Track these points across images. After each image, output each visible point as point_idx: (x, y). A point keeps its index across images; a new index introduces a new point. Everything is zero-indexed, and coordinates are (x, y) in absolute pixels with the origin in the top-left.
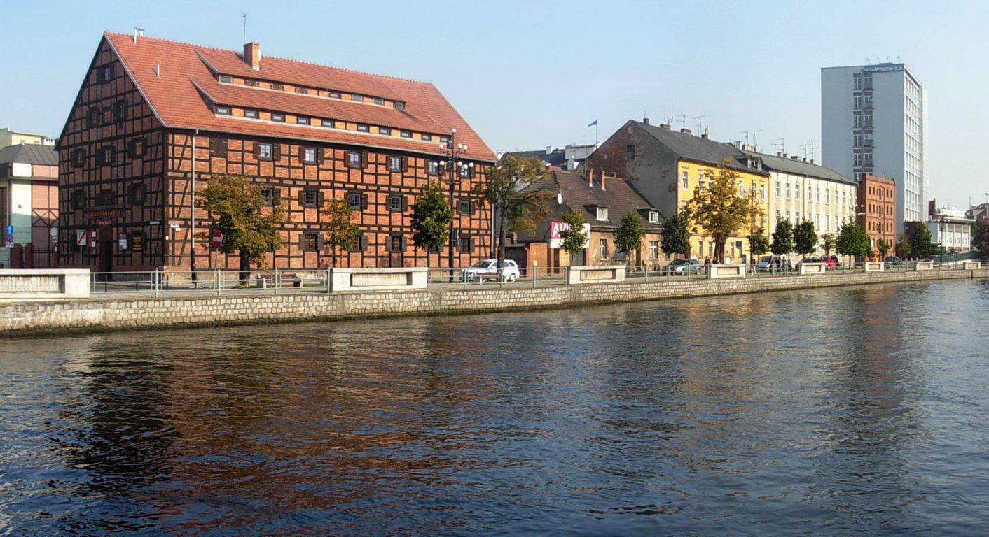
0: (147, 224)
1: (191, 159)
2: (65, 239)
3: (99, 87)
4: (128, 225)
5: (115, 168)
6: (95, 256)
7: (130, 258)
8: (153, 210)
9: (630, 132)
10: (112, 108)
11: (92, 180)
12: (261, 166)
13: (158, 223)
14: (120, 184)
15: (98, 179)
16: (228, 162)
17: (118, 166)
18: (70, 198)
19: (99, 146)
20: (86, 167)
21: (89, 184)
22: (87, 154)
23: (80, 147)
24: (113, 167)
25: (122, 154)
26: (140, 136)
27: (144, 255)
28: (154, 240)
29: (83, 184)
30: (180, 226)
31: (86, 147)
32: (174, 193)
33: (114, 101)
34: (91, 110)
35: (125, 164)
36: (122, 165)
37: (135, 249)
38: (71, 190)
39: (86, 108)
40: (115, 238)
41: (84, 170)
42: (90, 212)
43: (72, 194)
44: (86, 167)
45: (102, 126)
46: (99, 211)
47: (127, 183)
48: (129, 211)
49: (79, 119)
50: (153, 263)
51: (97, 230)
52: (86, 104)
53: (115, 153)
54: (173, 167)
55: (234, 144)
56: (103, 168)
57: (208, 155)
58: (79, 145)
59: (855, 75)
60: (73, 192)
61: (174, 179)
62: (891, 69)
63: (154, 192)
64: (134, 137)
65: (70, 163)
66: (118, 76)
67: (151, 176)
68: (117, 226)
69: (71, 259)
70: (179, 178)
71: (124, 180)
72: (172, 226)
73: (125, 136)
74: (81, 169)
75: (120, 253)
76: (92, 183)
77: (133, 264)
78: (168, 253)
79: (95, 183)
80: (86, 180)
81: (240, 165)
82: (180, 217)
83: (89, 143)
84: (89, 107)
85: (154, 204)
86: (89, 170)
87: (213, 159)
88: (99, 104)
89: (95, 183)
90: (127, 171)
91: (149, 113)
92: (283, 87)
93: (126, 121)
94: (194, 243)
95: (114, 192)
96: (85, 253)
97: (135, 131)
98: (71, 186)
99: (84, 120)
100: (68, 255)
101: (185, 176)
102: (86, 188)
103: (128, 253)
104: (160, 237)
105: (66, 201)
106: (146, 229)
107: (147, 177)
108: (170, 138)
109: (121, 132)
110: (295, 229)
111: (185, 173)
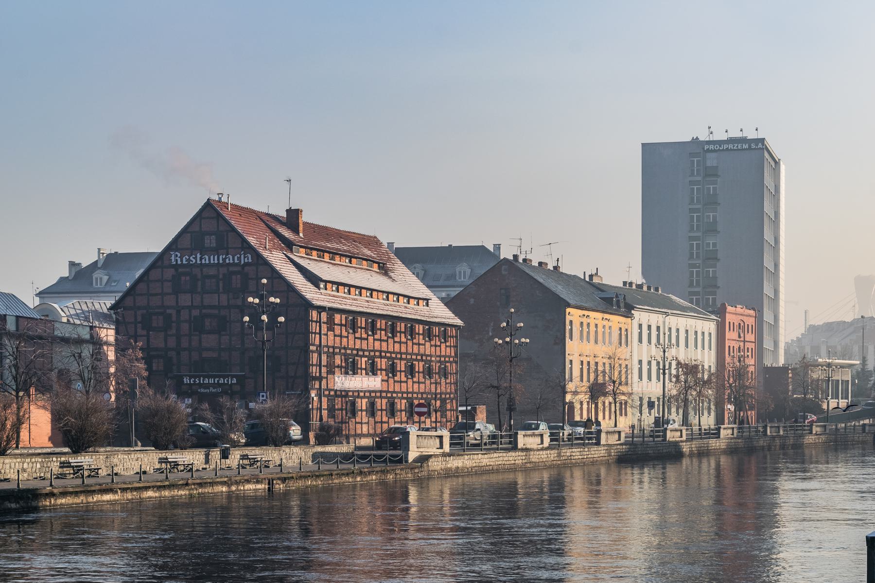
10: (221, 276)
11: (185, 343)
19: (196, 313)
20: (174, 331)
33: (223, 270)
39: (169, 273)
55: (337, 318)
56: (204, 336)
59: (692, 155)
61: (313, 352)
62: (746, 146)
84: (176, 270)
92: (323, 255)
102: (173, 354)
110: (364, 397)
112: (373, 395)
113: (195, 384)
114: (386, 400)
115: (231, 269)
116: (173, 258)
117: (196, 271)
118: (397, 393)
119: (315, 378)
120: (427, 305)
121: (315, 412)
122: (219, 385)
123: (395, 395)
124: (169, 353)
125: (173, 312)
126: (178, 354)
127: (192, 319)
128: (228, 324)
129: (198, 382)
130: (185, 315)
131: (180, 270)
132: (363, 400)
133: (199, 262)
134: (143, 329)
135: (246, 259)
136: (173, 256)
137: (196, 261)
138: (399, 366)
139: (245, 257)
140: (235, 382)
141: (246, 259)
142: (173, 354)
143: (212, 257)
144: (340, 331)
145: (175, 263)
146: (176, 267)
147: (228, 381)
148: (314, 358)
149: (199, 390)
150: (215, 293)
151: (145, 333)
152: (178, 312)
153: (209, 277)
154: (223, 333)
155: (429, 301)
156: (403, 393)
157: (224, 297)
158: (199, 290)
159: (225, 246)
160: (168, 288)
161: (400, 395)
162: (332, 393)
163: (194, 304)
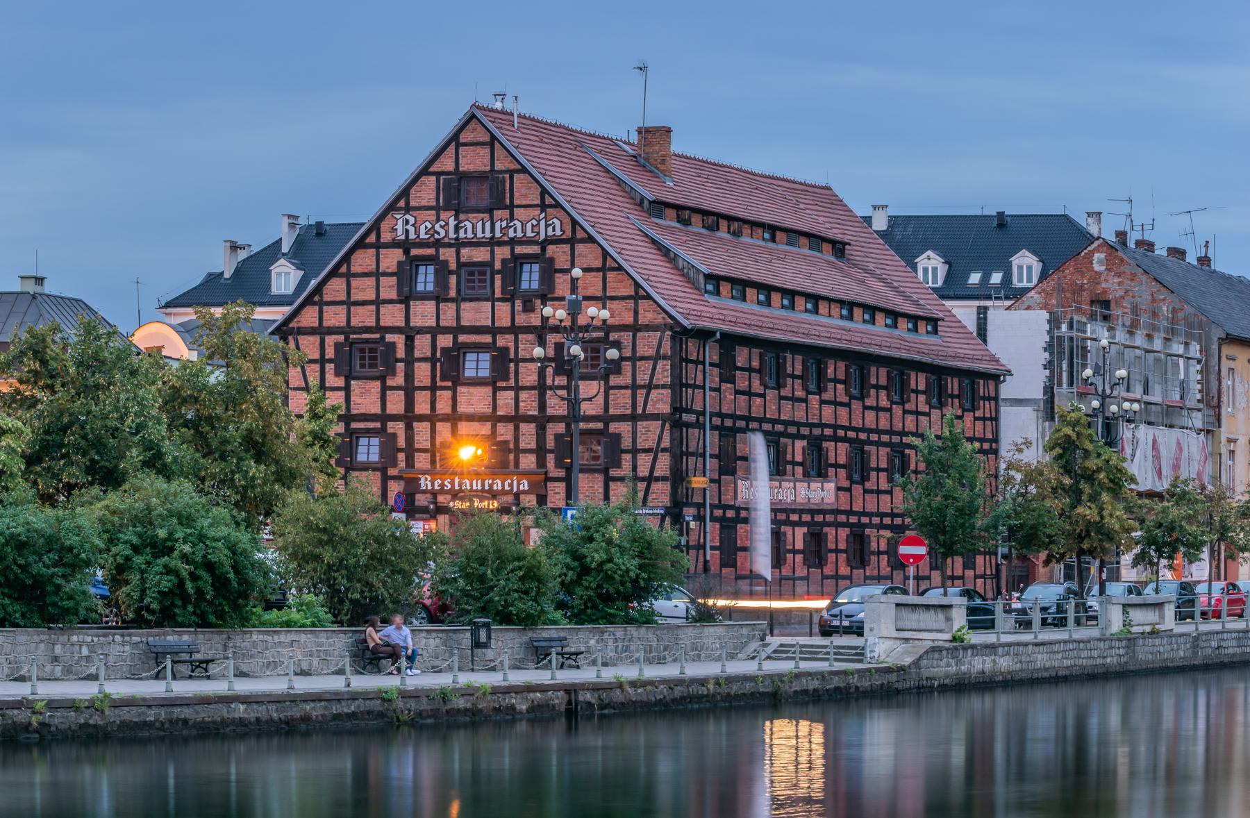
1: (703, 387)
8: (641, 486)
9: (1097, 267)
10: (498, 266)
11: (422, 407)
12: (768, 398)
13: (662, 512)
14: (528, 430)
17: (518, 389)
19: (445, 341)
20: (399, 380)
23: (377, 336)
26: (595, 335)
29: (384, 418)
33: (503, 253)
41: (384, 389)
45: (458, 300)
47: (550, 425)
51: (444, 519)
52: (395, 244)
53: (503, 363)
55: (742, 356)
56: (461, 390)
57: (717, 379)
61: (688, 425)
67: (633, 418)
72: (687, 518)
74: (378, 383)
81: (747, 397)
82: (695, 500)
84: (407, 252)
85: (643, 471)
86: (409, 390)
87: (724, 386)
94: (708, 552)
95: (506, 442)
102: (397, 428)
107: (621, 418)
109: (535, 321)
112: (819, 518)
113: (442, 491)
114: (847, 530)
115: (519, 250)
116: (399, 227)
117: (447, 254)
118: (870, 515)
120: (935, 331)
122: (494, 495)
124: (390, 424)
125: (399, 340)
126: (409, 428)
127: (438, 355)
128: (512, 365)
129: (449, 486)
130: (422, 345)
131: (414, 252)
133: (452, 235)
134: (337, 374)
135: (550, 229)
136: (400, 222)
137: (447, 232)
139: (547, 226)
140: (526, 488)
141: (550, 229)
142: (397, 428)
143: (480, 225)
144: (747, 383)
145: (403, 237)
146: (405, 245)
147: (511, 485)
149: (451, 504)
150: (487, 300)
151: (340, 382)
152: (410, 341)
154: (499, 384)
155: (939, 323)
156: (882, 515)
157: (503, 309)
158: (453, 293)
159: (508, 201)
160: (389, 288)
161: (876, 520)
162: (730, 514)
163: (442, 324)
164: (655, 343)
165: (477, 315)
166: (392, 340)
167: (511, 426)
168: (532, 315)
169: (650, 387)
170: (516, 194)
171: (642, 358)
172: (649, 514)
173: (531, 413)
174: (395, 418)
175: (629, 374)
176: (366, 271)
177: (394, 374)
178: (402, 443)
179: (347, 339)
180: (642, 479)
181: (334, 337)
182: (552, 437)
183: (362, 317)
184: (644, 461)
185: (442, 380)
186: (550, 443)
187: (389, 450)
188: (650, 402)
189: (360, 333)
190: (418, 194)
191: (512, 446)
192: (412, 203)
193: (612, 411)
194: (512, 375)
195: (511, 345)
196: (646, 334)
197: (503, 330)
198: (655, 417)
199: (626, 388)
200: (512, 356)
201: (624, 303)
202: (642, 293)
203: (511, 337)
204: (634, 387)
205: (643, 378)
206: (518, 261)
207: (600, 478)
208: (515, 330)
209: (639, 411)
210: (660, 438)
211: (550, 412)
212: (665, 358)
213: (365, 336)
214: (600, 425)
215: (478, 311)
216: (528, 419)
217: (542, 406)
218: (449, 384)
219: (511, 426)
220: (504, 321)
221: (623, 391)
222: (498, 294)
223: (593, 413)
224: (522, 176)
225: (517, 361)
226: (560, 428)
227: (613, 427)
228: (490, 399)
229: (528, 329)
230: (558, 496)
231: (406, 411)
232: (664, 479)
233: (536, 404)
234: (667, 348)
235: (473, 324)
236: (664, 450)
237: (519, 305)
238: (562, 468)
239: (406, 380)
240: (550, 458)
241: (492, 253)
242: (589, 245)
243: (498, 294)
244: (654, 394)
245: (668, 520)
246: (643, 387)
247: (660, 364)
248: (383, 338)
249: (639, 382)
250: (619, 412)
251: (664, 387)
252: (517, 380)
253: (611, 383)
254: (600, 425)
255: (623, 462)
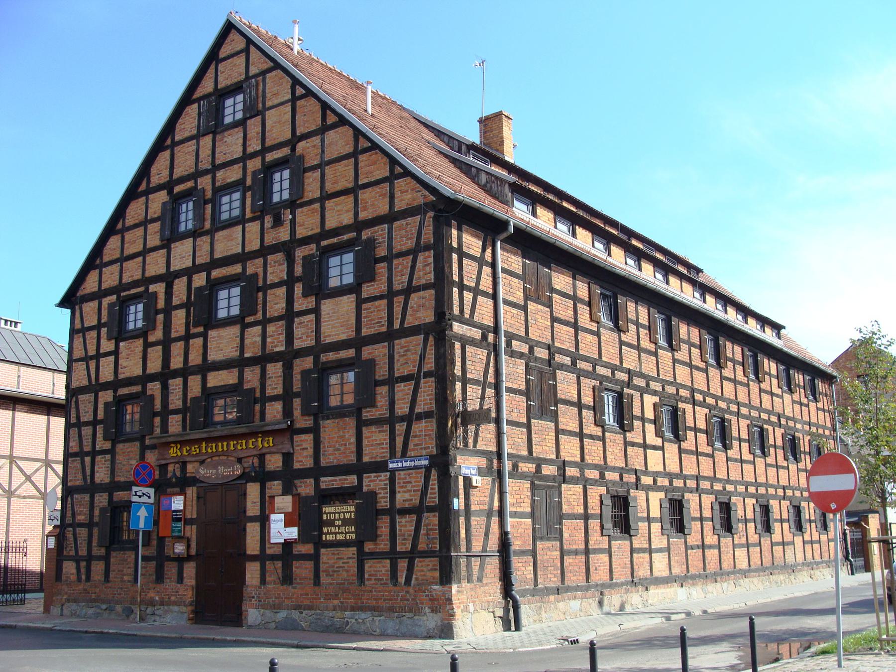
0: (379, 467)
2: (81, 518)
3: (207, 141)
4: (304, 474)
5: (258, 329)
6: (180, 560)
7: (310, 564)
8: (400, 428)
10: (249, 182)
11: (176, 362)
14: (275, 370)
15: (195, 358)
16: (554, 320)
17: (265, 322)
18: (101, 415)
19: (200, 280)
20: (157, 335)
21: (165, 375)
22: (161, 304)
23: (141, 289)
24: (245, 326)
25: (282, 291)
26: (345, 237)
27: (362, 558)
28: (404, 512)
29: (145, 379)
30: (480, 472)
31: (159, 288)
32: (465, 381)
33: (254, 164)
34: (177, 200)
35: (290, 316)
36: (279, 318)
37: (329, 537)
38: (107, 396)
40: (253, 509)
41: (147, 345)
42: (167, 445)
43: (107, 405)
44: (157, 335)
45: (211, 232)
46: (198, 441)
47: (297, 362)
48: (309, 438)
49: (136, 226)
50: (402, 580)
51: (191, 492)
52: (159, 188)
54: (462, 311)
56: (212, 334)
57: (521, 294)
58: (135, 284)
60: (110, 399)
63: (405, 379)
64: (324, 243)
65: (104, 330)
66: (269, 104)
67: (389, 336)
68: (263, 477)
69: (98, 568)
70: (473, 342)
71: (288, 358)
73: (287, 248)
74: (141, 341)
75: (269, 552)
76: (175, 374)
77: (324, 579)
78: (458, 549)
79: (185, 373)
80: (155, 365)
82: (481, 446)
83: (168, 278)
84: (170, 192)
85: (402, 408)
87: (531, 306)
88: (205, 182)
89: (185, 373)
90: (298, 332)
91: (382, 171)
93: (293, 204)
95: (253, 390)
96: (147, 553)
97: (331, 223)
98: (106, 386)
99: (154, 227)
100: (90, 558)
101: (484, 337)
102: (154, 388)
103: (308, 549)
104: (433, 497)
105: (87, 424)
106: (375, 482)
108: (454, 232)
109: (283, 234)
110: (655, 487)
111: (485, 330)
114: (712, 497)
117: (205, 182)
118: (735, 483)
119: (480, 417)
121: (477, 523)
123: (730, 488)
124: (150, 385)
125: (159, 288)
128: (260, 294)
132: (652, 494)
138: (734, 428)
148: (477, 359)
153: (229, 188)
156: (747, 485)
162: (549, 470)
164: (415, 231)
165: (229, 244)
166: (155, 290)
167: (257, 370)
168: (281, 229)
169: (409, 290)
170: (268, 95)
171: (401, 255)
172: (410, 468)
173: (277, 349)
174: (153, 378)
175: (385, 279)
176: (137, 221)
177: (154, 329)
178: (158, 406)
179: (118, 297)
180: (402, 419)
181: (109, 298)
182: (299, 377)
183: (133, 271)
184: (403, 391)
185: (195, 326)
186: (297, 386)
187: (148, 414)
188: (409, 312)
189: (129, 289)
190: (182, 127)
191: (258, 394)
192: (178, 138)
193: (365, 332)
194: (260, 307)
195: (260, 271)
196: (403, 222)
197: (254, 255)
198: (414, 331)
199: (381, 297)
200: (260, 284)
201: (377, 189)
202: (398, 170)
203: (259, 261)
204: (390, 295)
205: (400, 281)
206: (269, 169)
207: (351, 422)
208: (264, 251)
209: (397, 325)
210: (422, 357)
211: (298, 344)
212: (427, 248)
213: (133, 291)
214: (351, 353)
215: (229, 238)
216: (274, 357)
217: (290, 338)
218: (201, 329)
219: (257, 370)
220: (254, 245)
221: (377, 303)
222: (248, 215)
223: (343, 337)
224: (274, 73)
225: (266, 288)
226: (307, 363)
227: (367, 352)
228: (238, 339)
229: (275, 249)
230: (305, 453)
231: (163, 368)
232: (428, 415)
233: (283, 338)
234: (428, 235)
235: (225, 254)
236: (427, 375)
237: (268, 220)
238: (309, 415)
239: (164, 333)
240: (297, 402)
241: (245, 168)
242: (341, 129)
243: (248, 215)
244: (414, 298)
245: (434, 474)
246: (399, 293)
247: (421, 258)
248: (147, 289)
249: (397, 287)
250: (372, 331)
251: (426, 287)
252: (264, 313)
253: (364, 295)
254: (351, 353)
255: (379, 398)
